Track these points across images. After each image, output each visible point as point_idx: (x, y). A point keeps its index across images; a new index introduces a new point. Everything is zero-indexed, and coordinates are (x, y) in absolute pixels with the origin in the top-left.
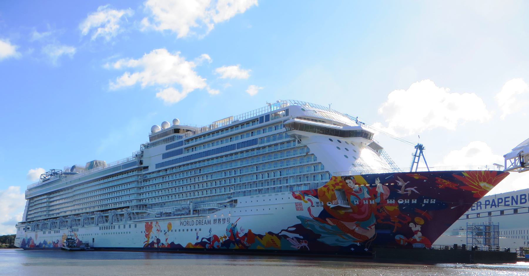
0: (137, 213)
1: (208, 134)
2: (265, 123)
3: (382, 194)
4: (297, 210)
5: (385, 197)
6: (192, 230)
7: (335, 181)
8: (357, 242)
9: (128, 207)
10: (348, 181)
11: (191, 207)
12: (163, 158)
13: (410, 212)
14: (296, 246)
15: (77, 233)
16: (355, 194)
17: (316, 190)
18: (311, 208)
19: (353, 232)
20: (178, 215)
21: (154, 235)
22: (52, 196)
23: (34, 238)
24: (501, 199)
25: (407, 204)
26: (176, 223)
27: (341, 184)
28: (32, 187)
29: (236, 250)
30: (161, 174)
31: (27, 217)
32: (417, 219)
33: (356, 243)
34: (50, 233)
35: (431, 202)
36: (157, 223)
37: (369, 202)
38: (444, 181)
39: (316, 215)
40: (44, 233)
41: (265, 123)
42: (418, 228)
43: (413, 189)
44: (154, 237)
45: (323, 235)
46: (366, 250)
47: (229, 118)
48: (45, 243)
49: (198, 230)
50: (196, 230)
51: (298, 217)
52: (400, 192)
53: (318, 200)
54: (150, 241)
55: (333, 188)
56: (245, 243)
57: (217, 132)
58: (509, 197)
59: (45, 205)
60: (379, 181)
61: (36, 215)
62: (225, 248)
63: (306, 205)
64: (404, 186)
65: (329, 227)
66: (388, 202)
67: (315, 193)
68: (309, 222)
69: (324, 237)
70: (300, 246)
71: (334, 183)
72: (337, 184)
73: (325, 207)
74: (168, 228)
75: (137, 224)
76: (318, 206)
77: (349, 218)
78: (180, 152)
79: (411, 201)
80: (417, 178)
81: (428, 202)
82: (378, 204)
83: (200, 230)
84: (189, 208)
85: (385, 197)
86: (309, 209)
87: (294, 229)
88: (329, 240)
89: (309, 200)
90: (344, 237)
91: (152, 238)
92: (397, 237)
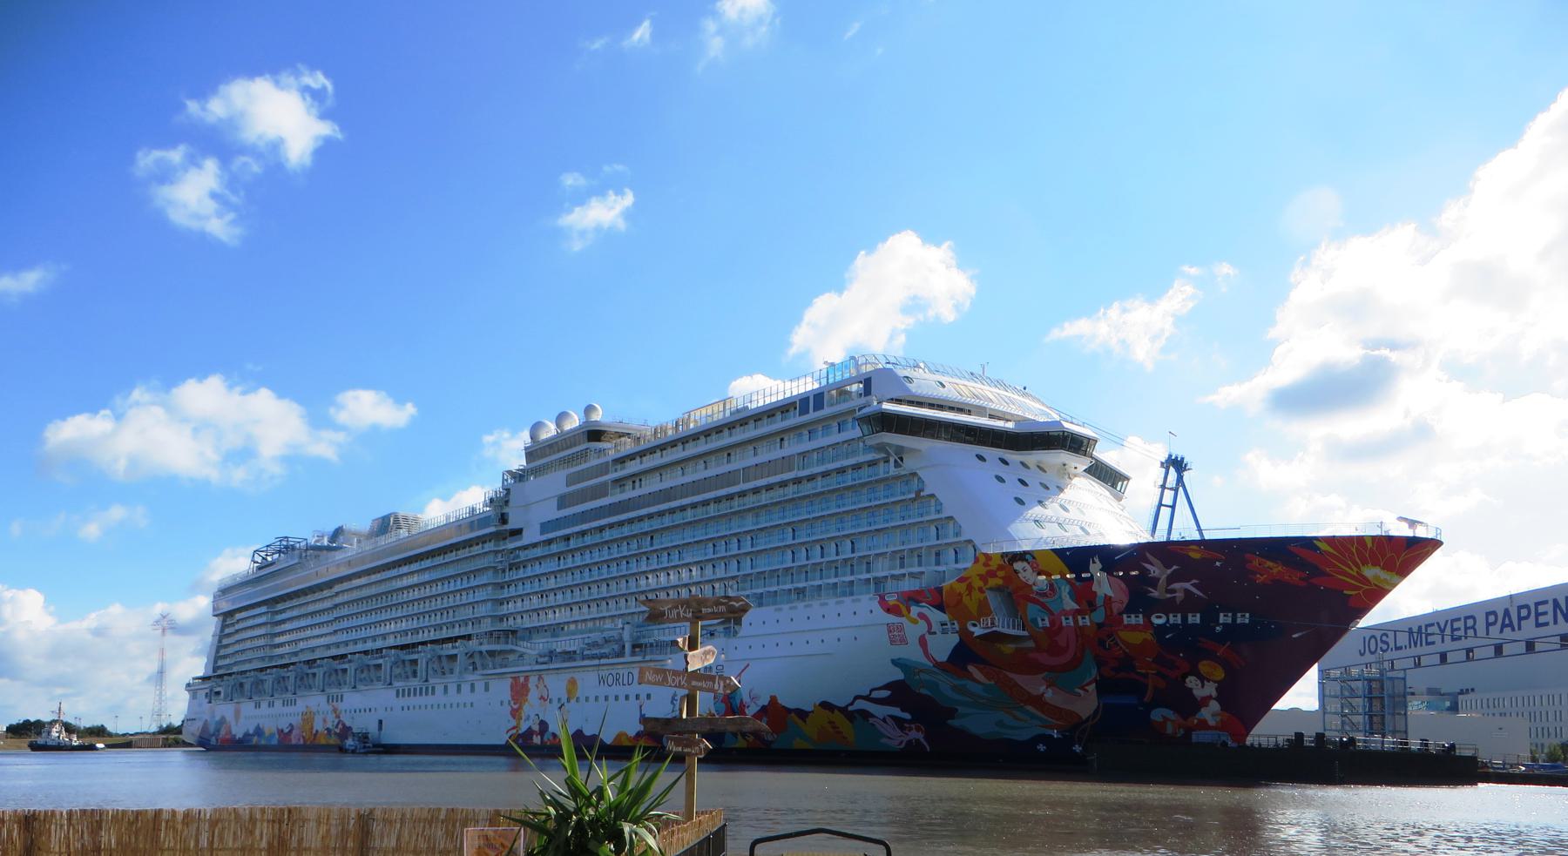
0: (492, 653)
1: (673, 444)
2: (812, 415)
3: (1107, 599)
4: (892, 642)
5: (1116, 608)
6: (627, 697)
7: (986, 565)
8: (1052, 727)
9: (469, 637)
10: (1018, 566)
11: (626, 636)
12: (560, 507)
13: (1183, 648)
14: (895, 739)
15: (341, 706)
16: (1041, 599)
17: (939, 590)
18: (928, 637)
19: (1038, 701)
20: (593, 657)
21: (533, 710)
22: (280, 607)
23: (230, 717)
24: (1527, 607)
25: (1175, 626)
26: (588, 681)
28: (230, 583)
29: (740, 751)
30: (554, 548)
31: (215, 662)
32: (1204, 667)
33: (1049, 732)
34: (271, 705)
35: (1239, 621)
36: (540, 678)
37: (1076, 621)
38: (1269, 564)
39: (943, 657)
40: (258, 705)
41: (812, 415)
42: (1210, 689)
43: (1187, 585)
44: (532, 716)
45: (961, 709)
46: (1078, 748)
47: (724, 402)
48: (259, 731)
49: (643, 697)
50: (637, 697)
51: (893, 662)
52: (1155, 594)
53: (944, 617)
54: (523, 728)
55: (981, 584)
57: (695, 437)
58: (1545, 602)
59: (262, 631)
60: (1099, 565)
61: (239, 658)
63: (914, 630)
64: (1164, 577)
66: (1126, 620)
67: (938, 599)
68: (924, 676)
70: (906, 739)
71: (983, 570)
72: (992, 574)
73: (964, 634)
74: (569, 692)
75: (492, 684)
76: (944, 632)
77: (1025, 664)
78: (599, 491)
79: (1185, 619)
80: (1195, 556)
81: (1229, 620)
82: (1100, 626)
83: (649, 697)
84: (621, 639)
85: (1116, 608)
86: (923, 641)
87: (885, 694)
88: (978, 723)
89: (922, 616)
90: (1018, 714)
91: (528, 718)
92: (1157, 715)
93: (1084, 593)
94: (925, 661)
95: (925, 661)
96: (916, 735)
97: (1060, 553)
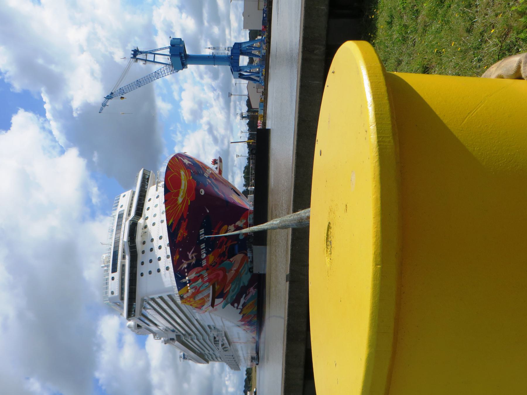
8: (247, 261)
10: (185, 297)
14: (253, 291)
19: (237, 271)
27: (188, 299)
38: (179, 235)
39: (222, 299)
45: (242, 285)
51: (224, 307)
62: (256, 324)
65: (233, 286)
68: (229, 300)
69: (243, 283)
80: (178, 257)
82: (207, 270)
85: (199, 269)
88: (246, 278)
93: (195, 280)
94: (223, 303)
95: (223, 303)
96: (251, 289)
97: (179, 290)
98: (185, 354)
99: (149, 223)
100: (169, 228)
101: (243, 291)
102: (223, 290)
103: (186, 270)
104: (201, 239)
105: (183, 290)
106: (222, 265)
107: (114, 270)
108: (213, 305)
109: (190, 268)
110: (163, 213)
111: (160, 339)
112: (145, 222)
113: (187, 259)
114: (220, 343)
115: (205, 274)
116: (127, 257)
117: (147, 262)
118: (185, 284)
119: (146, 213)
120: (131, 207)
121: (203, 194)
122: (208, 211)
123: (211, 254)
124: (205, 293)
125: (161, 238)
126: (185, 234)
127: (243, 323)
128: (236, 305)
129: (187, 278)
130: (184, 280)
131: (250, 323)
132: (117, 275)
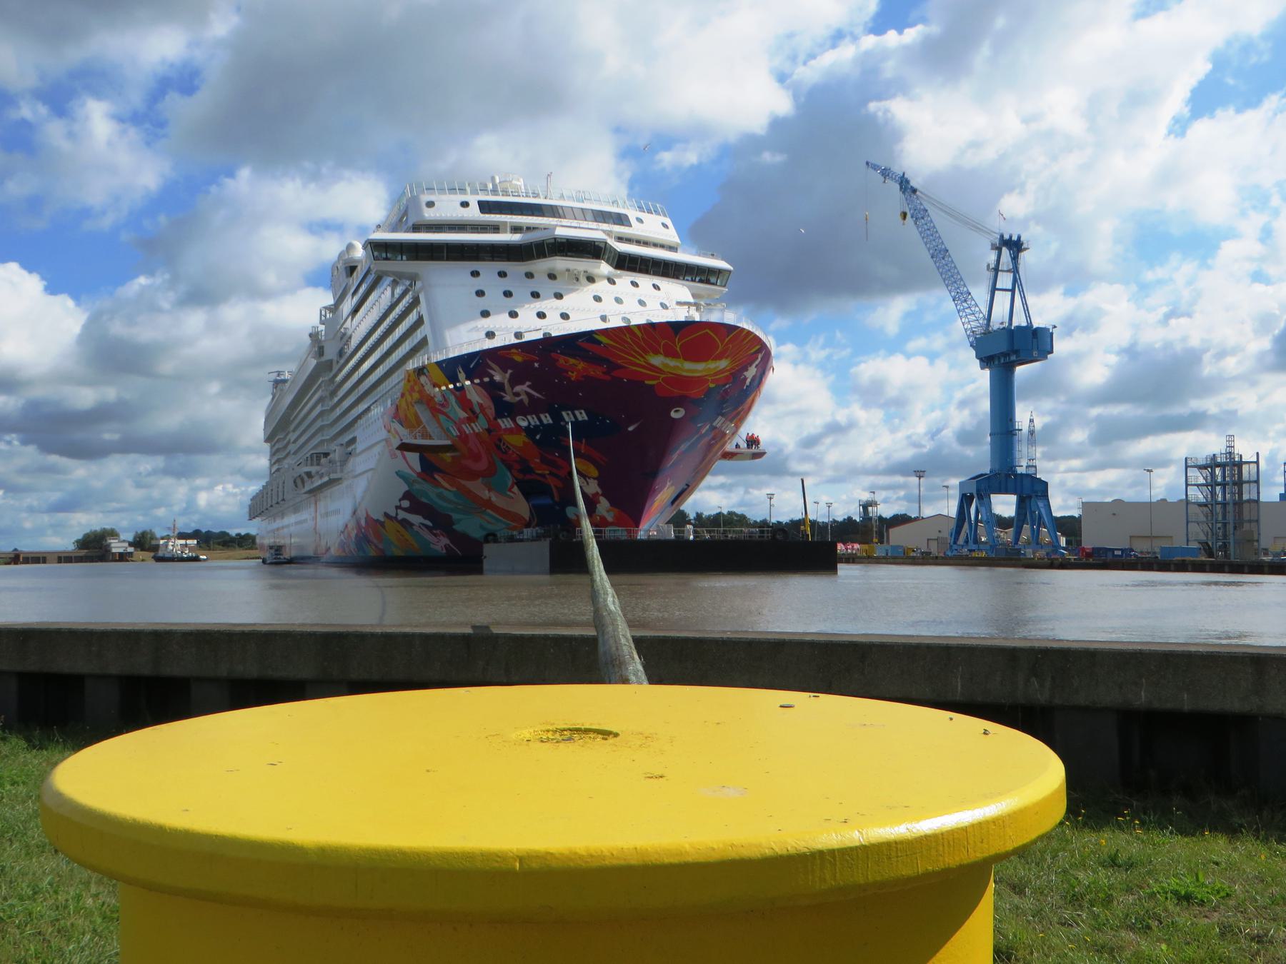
3: (480, 405)
8: (514, 528)
10: (423, 379)
14: (439, 544)
19: (488, 504)
27: (416, 388)
38: (572, 361)
39: (418, 469)
45: (455, 516)
56: (375, 541)
68: (417, 486)
80: (518, 359)
82: (489, 431)
85: (491, 412)
87: (406, 504)
88: (471, 526)
93: (465, 403)
94: (409, 471)
95: (409, 471)
96: (445, 541)
97: (439, 364)
98: (287, 385)
99: (601, 287)
100: (589, 336)
101: (440, 522)
102: (439, 471)
103: (486, 379)
104: (564, 413)
105: (438, 375)
106: (502, 468)
107: (485, 207)
108: (404, 447)
109: (493, 389)
110: (624, 319)
111: (322, 323)
112: (602, 277)
113: (514, 381)
114: (313, 469)
115: (480, 426)
116: (516, 238)
117: (506, 284)
118: (453, 379)
119: (625, 279)
120: (638, 242)
121: (673, 415)
122: (631, 429)
123: (526, 440)
124: (432, 428)
125: (565, 316)
126: (573, 376)
127: (363, 523)
128: (406, 504)
129: (468, 383)
130: (462, 376)
131: (362, 539)
132: (473, 213)
